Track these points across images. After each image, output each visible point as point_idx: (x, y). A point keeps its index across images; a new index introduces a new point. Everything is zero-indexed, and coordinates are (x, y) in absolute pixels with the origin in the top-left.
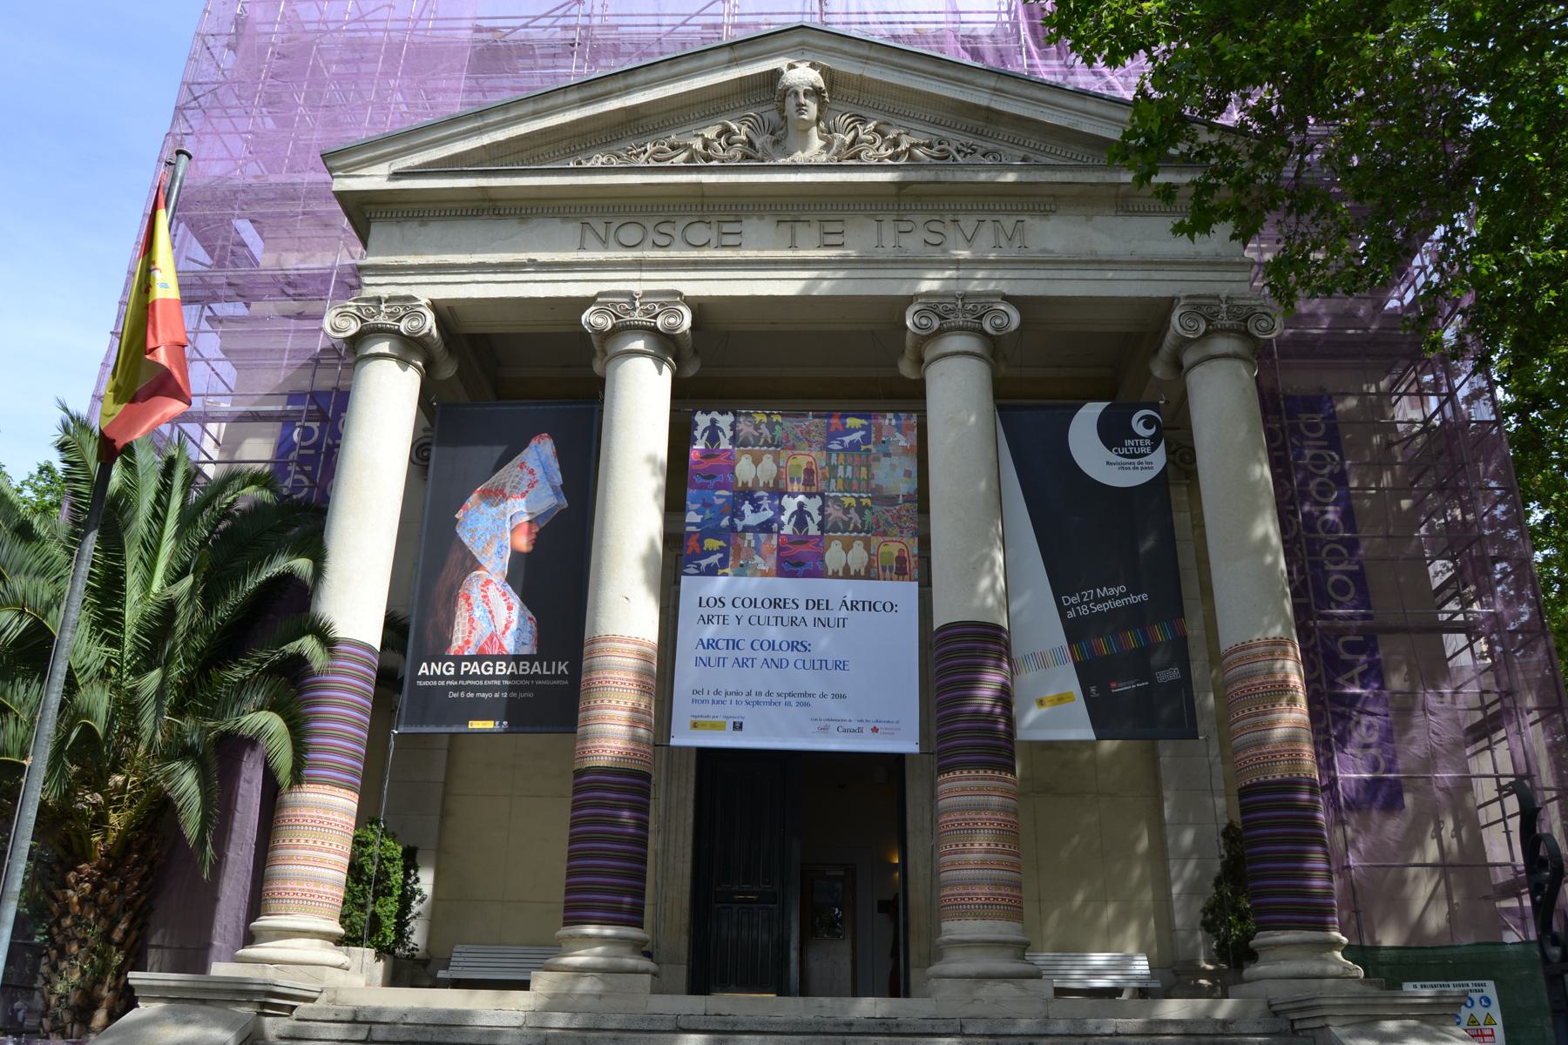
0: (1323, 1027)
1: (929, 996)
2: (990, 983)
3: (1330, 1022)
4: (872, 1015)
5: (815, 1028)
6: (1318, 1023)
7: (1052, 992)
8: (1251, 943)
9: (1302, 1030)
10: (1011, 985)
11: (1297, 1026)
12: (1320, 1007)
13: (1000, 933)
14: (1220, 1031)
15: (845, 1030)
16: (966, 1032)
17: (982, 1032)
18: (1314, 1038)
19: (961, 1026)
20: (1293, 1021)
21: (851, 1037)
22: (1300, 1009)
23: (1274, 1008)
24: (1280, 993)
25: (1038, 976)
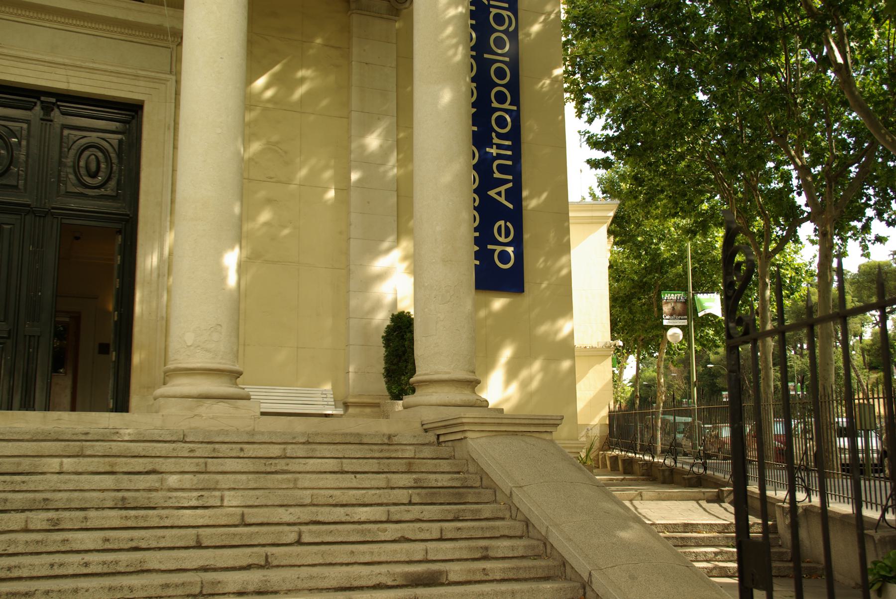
0: (462, 439)
1: (157, 412)
2: (209, 401)
3: (468, 434)
4: (107, 426)
5: (55, 437)
6: (459, 436)
7: (258, 414)
8: (412, 380)
9: (445, 442)
10: (226, 405)
11: (442, 439)
12: (462, 424)
13: (220, 363)
14: (386, 441)
15: (83, 438)
16: (188, 440)
17: (201, 440)
18: (453, 447)
19: (184, 435)
20: (438, 436)
21: (88, 443)
22: (445, 427)
23: (425, 427)
24: (430, 416)
25: (247, 398)
